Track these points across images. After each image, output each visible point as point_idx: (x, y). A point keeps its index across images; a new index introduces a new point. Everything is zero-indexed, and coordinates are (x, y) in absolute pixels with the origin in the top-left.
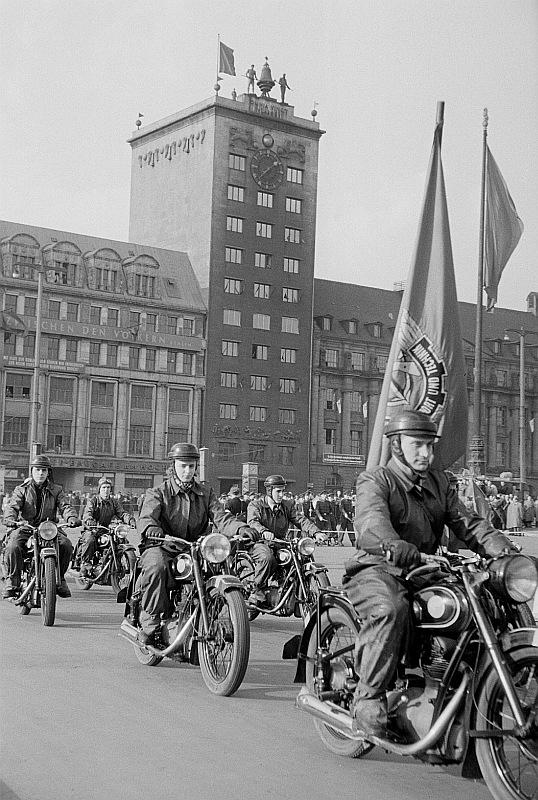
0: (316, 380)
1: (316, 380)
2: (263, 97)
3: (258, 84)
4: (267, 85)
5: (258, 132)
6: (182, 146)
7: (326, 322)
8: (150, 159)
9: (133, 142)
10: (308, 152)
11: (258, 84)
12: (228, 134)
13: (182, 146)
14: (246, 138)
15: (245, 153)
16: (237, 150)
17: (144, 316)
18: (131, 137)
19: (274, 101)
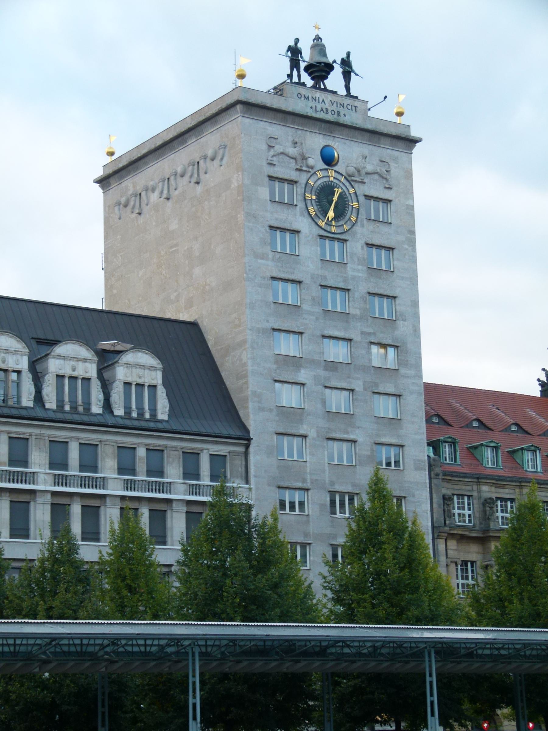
0: (441, 546)
1: (441, 546)
2: (314, 87)
3: (306, 69)
4: (320, 71)
6: (188, 175)
7: (447, 450)
8: (133, 204)
9: (103, 182)
10: (395, 171)
11: (306, 69)
12: (264, 147)
13: (188, 175)
14: (292, 151)
15: (293, 175)
16: (278, 172)
17: (141, 452)
18: (99, 173)
19: (335, 93)
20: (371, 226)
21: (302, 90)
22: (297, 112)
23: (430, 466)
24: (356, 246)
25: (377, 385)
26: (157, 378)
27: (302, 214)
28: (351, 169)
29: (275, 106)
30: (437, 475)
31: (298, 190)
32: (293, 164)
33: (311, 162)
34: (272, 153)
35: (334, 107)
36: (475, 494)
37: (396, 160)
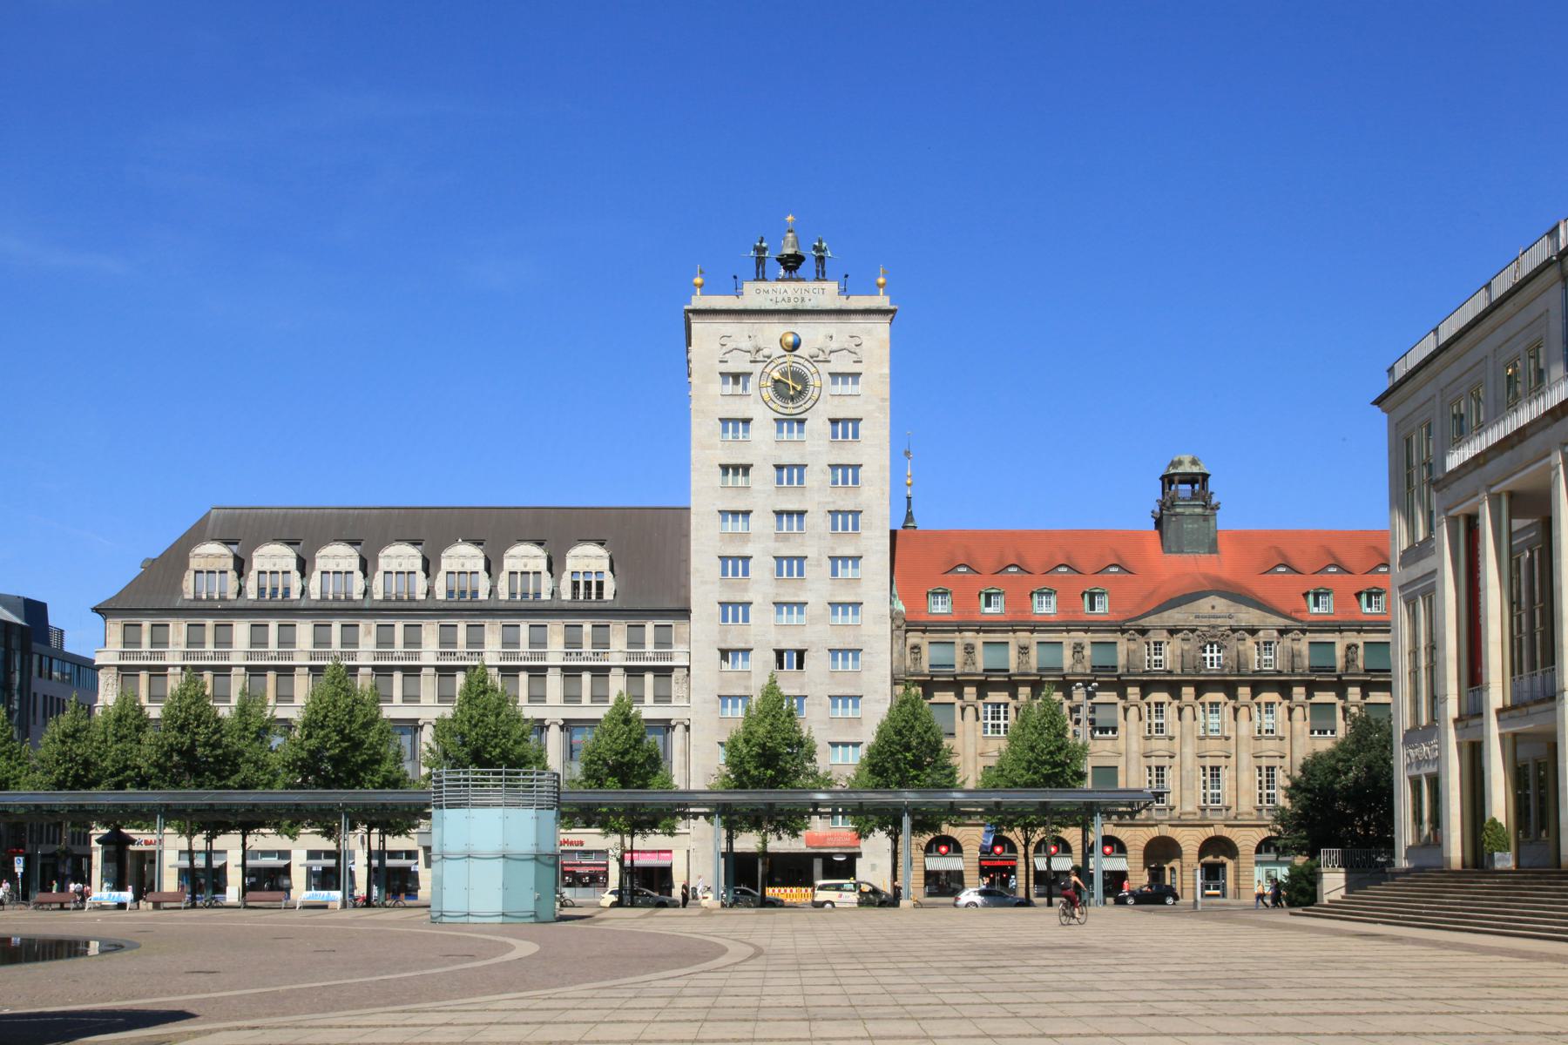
5: (772, 333)
15: (747, 368)
20: (836, 400)
21: (762, 285)
22: (750, 307)
23: (893, 619)
24: (817, 423)
25: (832, 549)
26: (605, 565)
27: (756, 402)
28: (814, 351)
29: (724, 307)
30: (899, 627)
31: (753, 380)
32: (748, 357)
33: (766, 352)
34: (725, 349)
35: (798, 295)
36: (958, 641)
37: (869, 333)
